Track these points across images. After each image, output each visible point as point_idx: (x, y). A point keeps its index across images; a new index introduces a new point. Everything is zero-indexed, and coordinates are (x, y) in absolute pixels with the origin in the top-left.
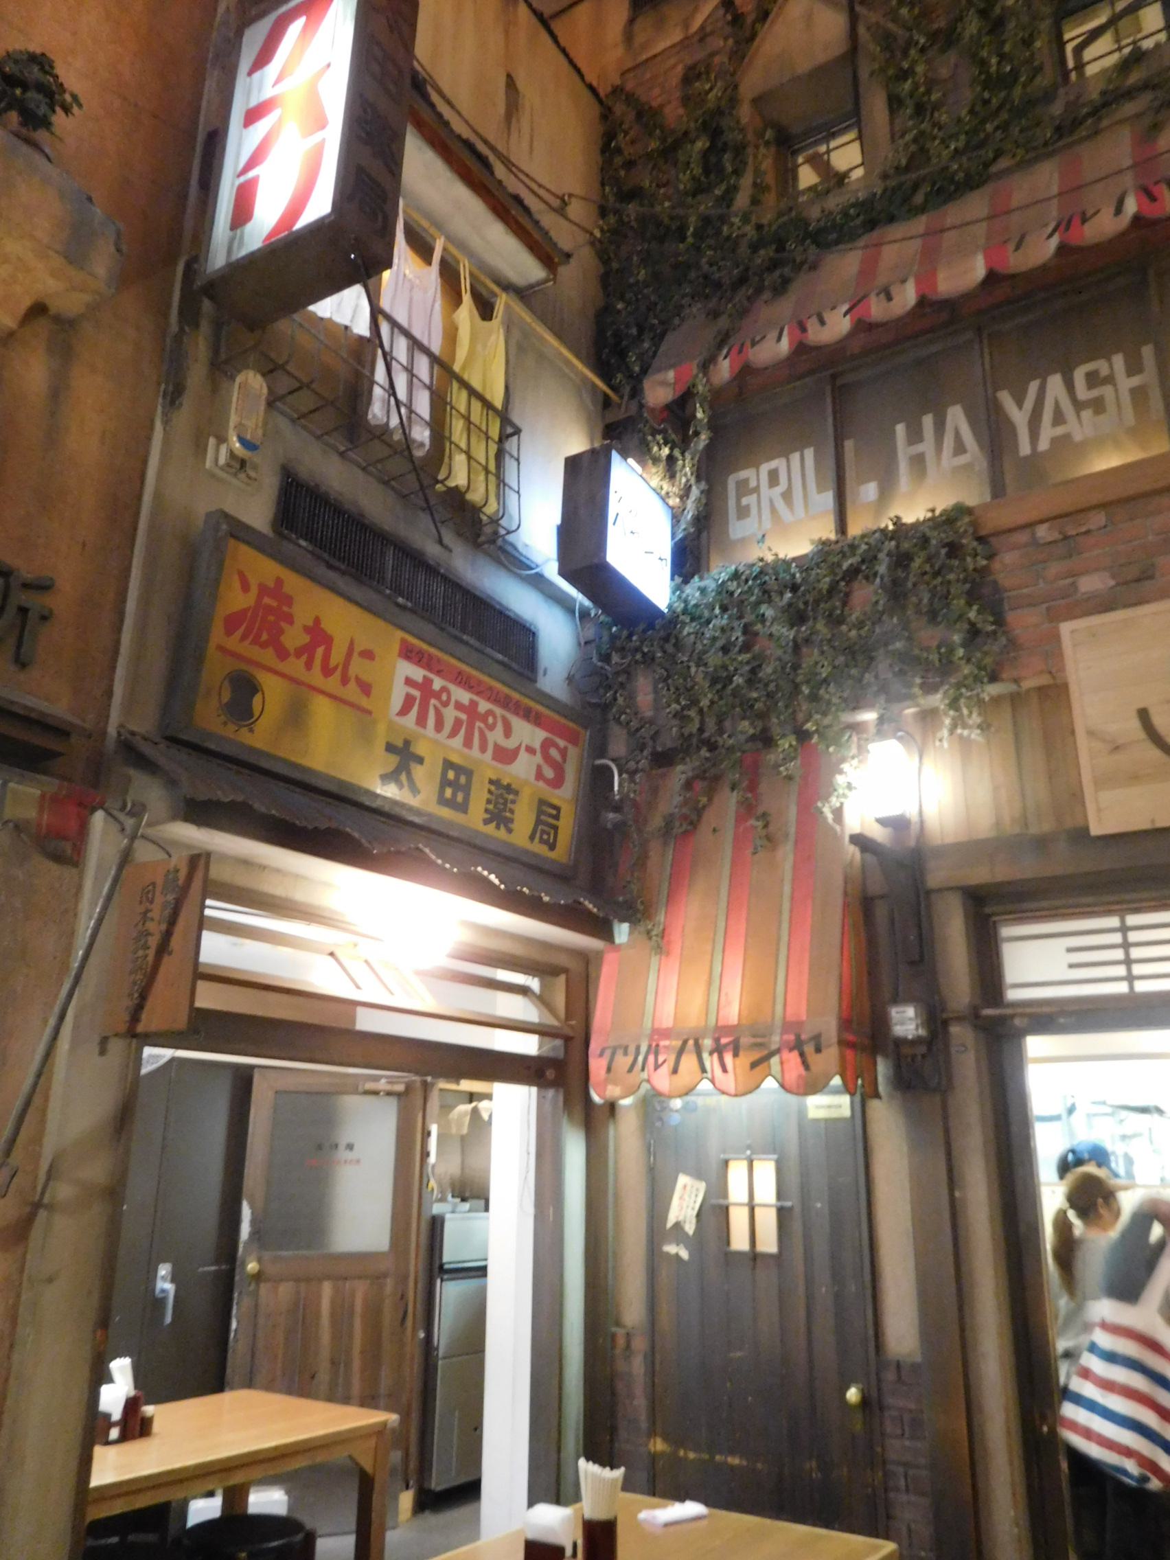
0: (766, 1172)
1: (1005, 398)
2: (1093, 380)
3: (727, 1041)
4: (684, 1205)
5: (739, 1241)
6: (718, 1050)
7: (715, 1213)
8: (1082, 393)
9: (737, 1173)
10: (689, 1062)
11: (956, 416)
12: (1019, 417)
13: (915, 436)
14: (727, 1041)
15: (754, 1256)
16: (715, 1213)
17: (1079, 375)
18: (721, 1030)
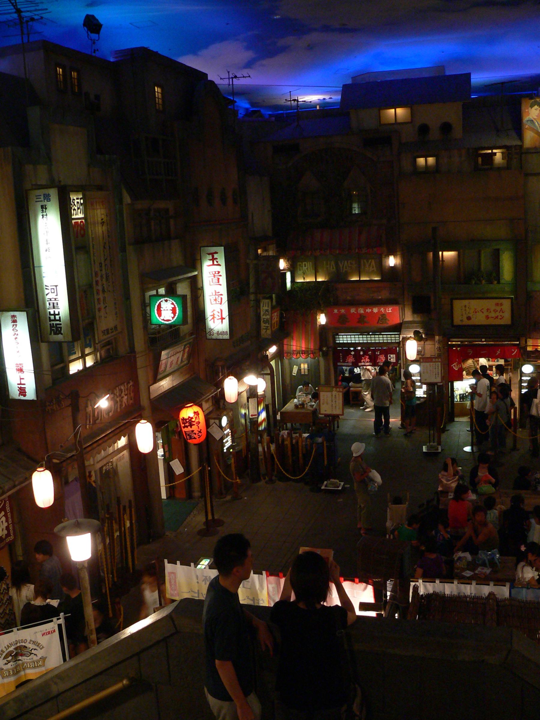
0: (306, 366)
1: (339, 262)
2: (351, 264)
3: (303, 352)
4: (295, 369)
5: (303, 373)
6: (302, 353)
7: (299, 370)
8: (350, 265)
9: (302, 366)
10: (298, 355)
11: (333, 263)
12: (341, 266)
13: (327, 265)
14: (303, 352)
15: (305, 375)
16: (299, 370)
17: (349, 262)
18: (303, 351)
